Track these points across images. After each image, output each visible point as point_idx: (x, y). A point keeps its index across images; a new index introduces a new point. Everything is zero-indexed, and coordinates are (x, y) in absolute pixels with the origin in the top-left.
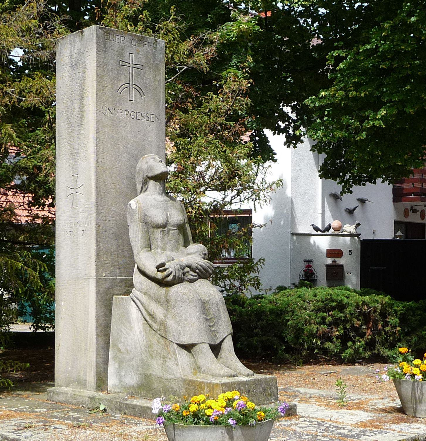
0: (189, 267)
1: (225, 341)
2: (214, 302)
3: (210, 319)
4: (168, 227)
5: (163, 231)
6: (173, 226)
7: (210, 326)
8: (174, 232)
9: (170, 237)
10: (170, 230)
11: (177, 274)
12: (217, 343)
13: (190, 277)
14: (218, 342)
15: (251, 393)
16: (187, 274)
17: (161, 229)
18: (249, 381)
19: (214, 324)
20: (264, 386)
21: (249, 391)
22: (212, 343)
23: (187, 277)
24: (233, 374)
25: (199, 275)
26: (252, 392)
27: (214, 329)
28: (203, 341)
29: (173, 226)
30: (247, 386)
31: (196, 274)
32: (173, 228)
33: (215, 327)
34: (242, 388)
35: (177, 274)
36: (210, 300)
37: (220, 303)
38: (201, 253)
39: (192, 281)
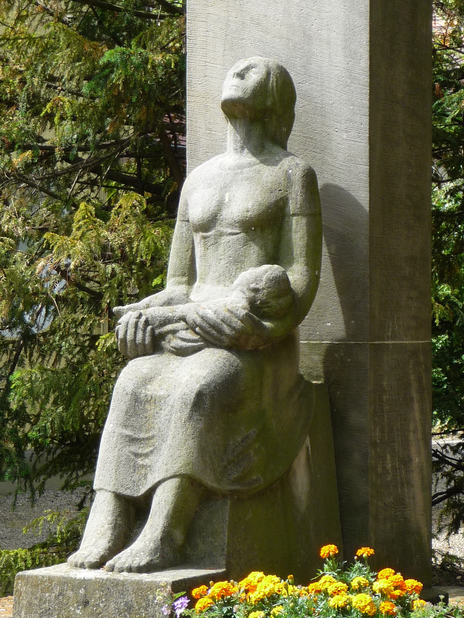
0: (183, 319)
1: (159, 491)
2: (171, 403)
3: (148, 439)
4: (218, 228)
5: (204, 238)
6: (231, 225)
7: (137, 455)
8: (230, 241)
9: (221, 248)
10: (221, 234)
11: (129, 337)
12: (140, 494)
13: (176, 343)
14: (143, 490)
15: (89, 609)
16: (170, 336)
17: (201, 234)
18: (89, 580)
19: (152, 452)
20: (131, 597)
21: (86, 603)
22: (128, 493)
23: (169, 342)
24: (80, 562)
25: (203, 339)
26: (93, 606)
27: (140, 461)
28: (102, 486)
29: (231, 225)
30: (82, 591)
31: (197, 337)
32: (230, 231)
33: (151, 457)
34: (70, 593)
35: (129, 337)
36: (169, 396)
37: (178, 405)
38: (245, 289)
39: (182, 352)
